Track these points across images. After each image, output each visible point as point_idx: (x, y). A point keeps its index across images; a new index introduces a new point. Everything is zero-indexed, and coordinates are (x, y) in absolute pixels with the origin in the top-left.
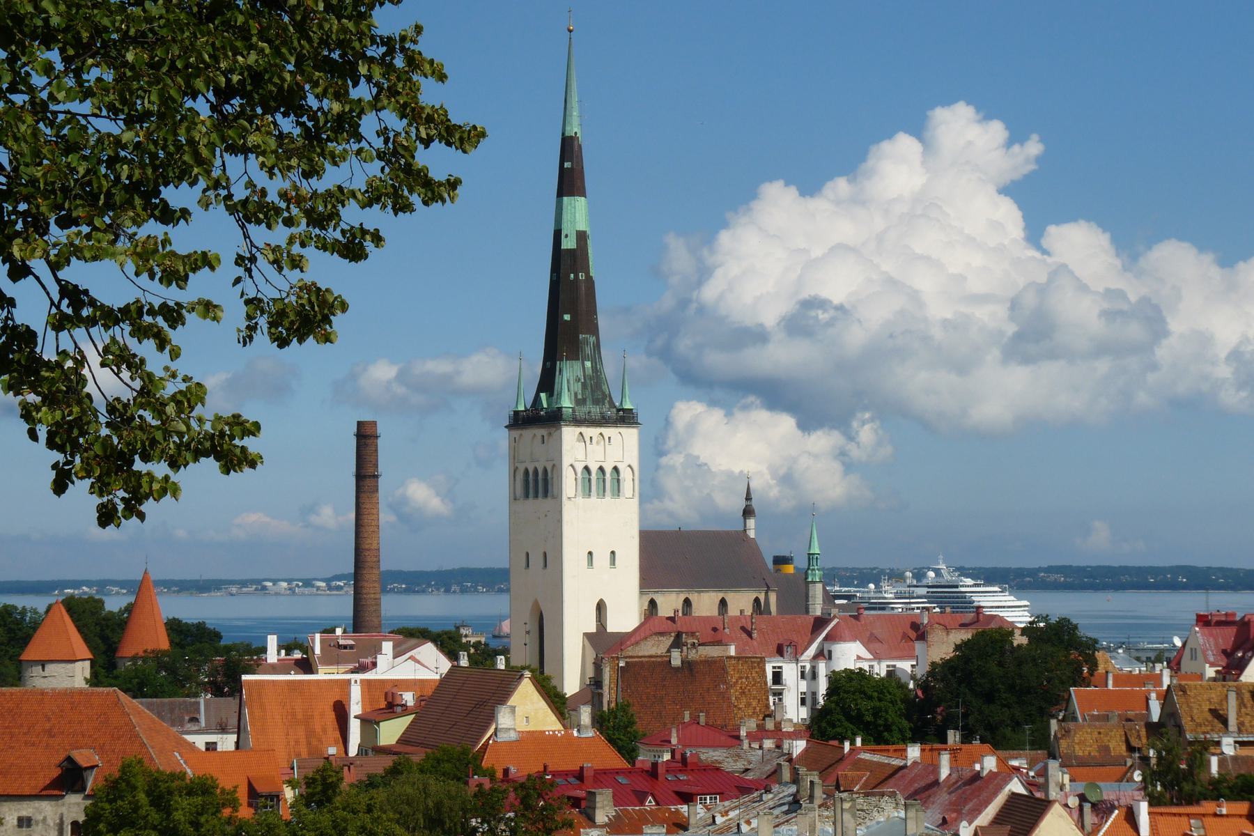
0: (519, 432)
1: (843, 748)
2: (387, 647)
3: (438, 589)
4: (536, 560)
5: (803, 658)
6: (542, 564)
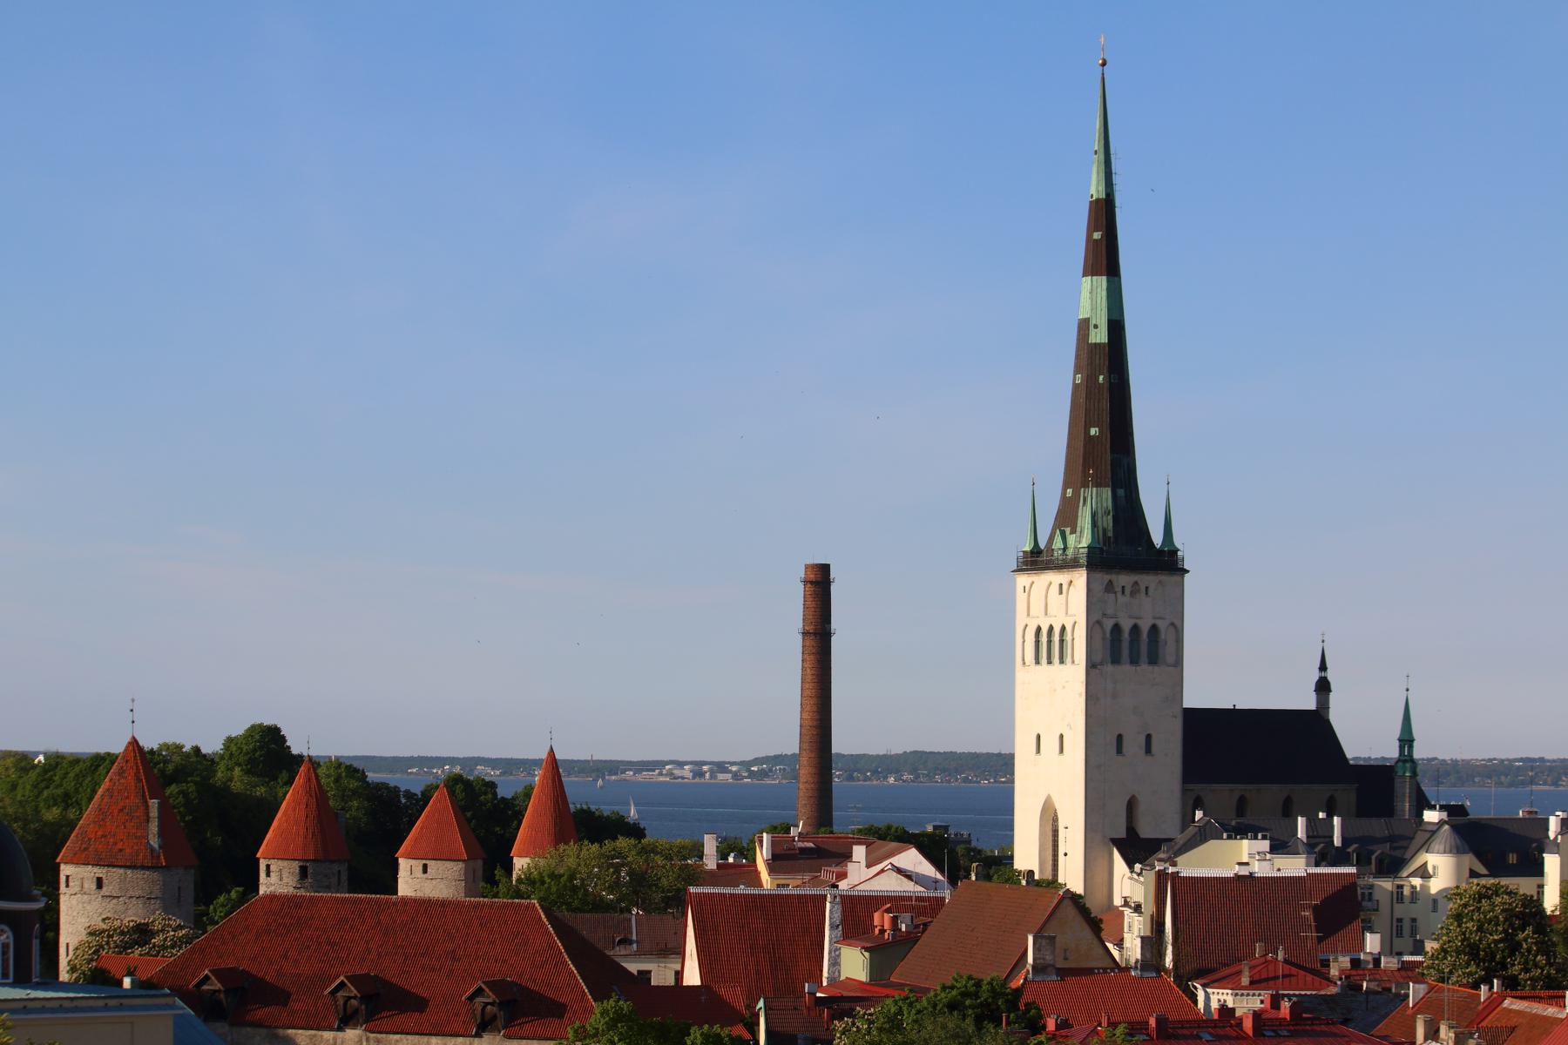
2: (859, 852)
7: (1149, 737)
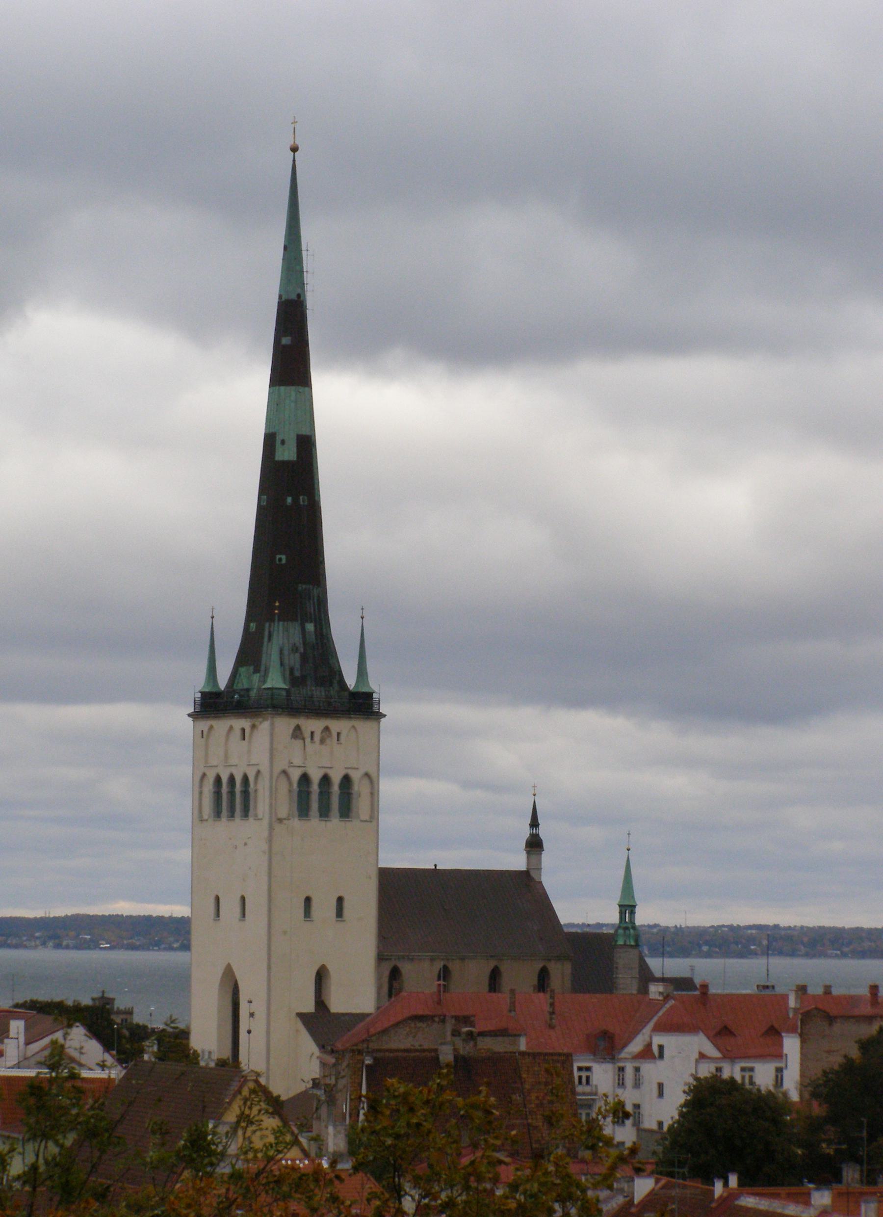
1: (713, 1192)
2: (17, 1027)
3: (44, 944)
5: (623, 1055)
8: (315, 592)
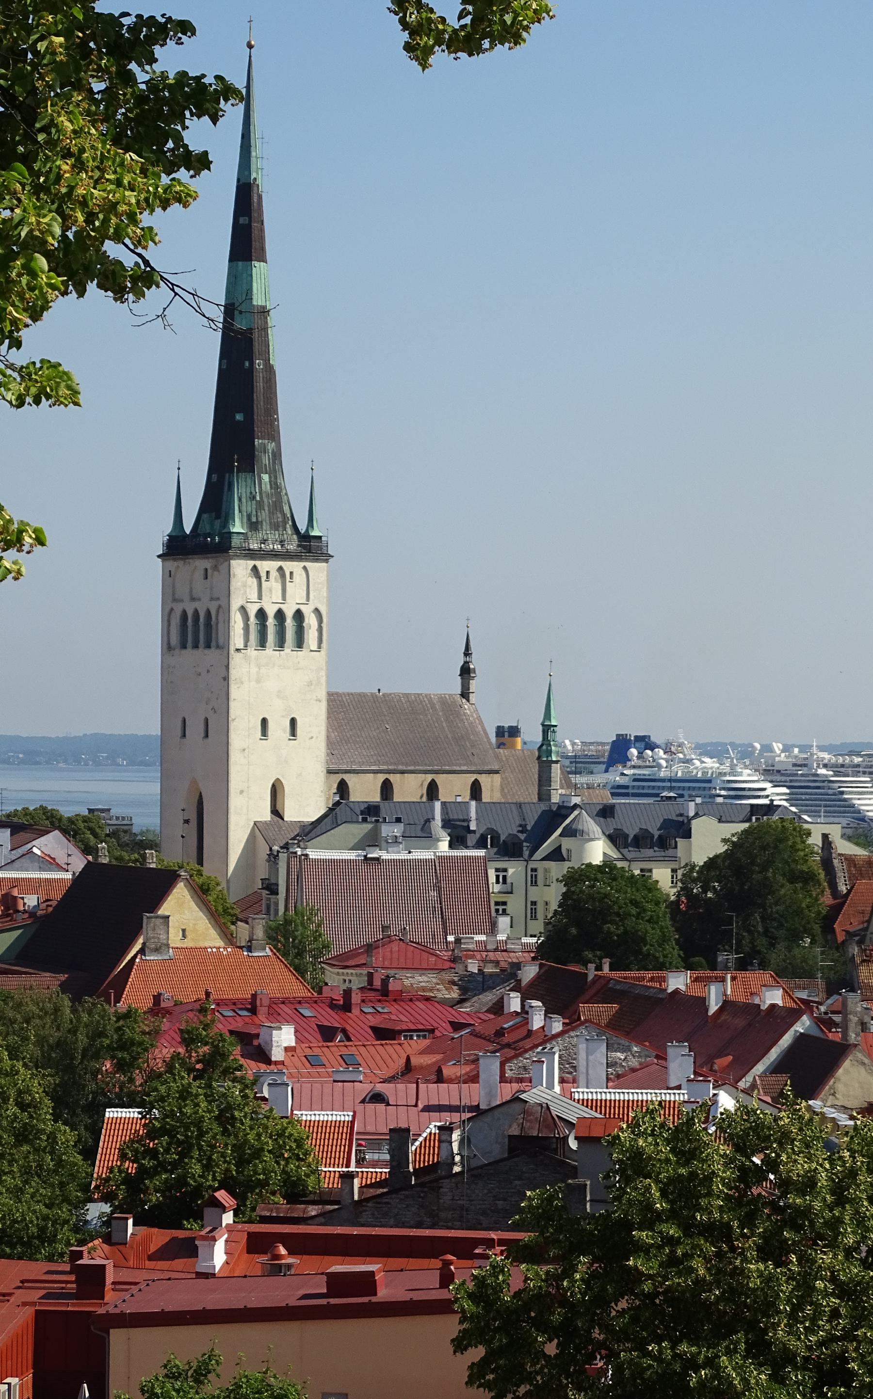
0: (176, 564)
4: (195, 729)
6: (203, 735)
7: (293, 722)
8: (271, 446)
